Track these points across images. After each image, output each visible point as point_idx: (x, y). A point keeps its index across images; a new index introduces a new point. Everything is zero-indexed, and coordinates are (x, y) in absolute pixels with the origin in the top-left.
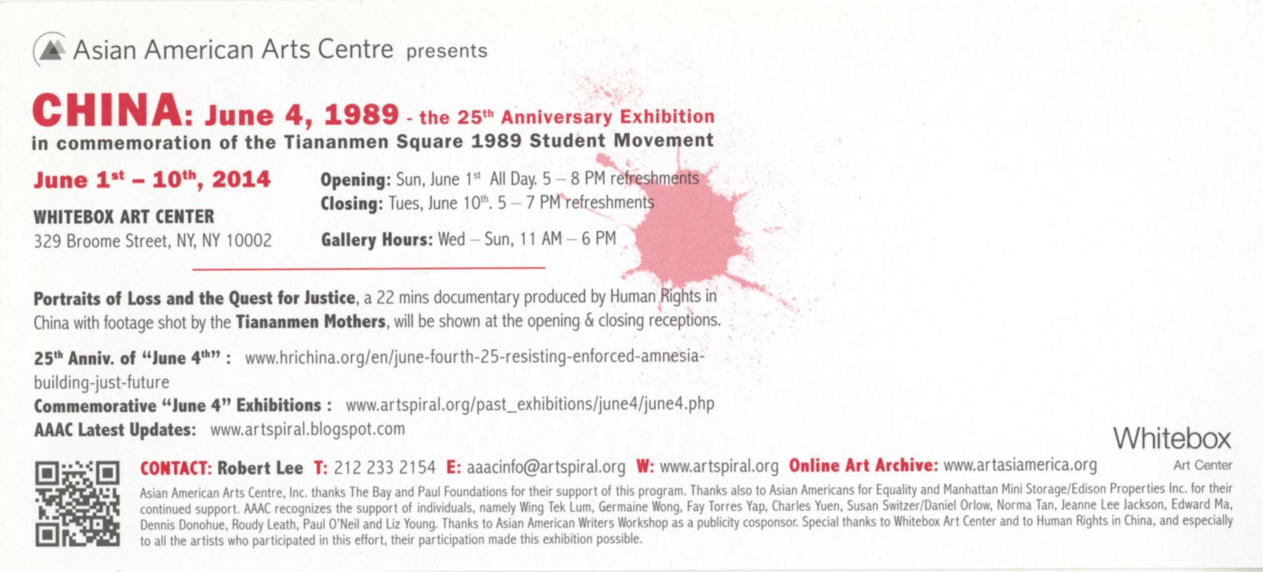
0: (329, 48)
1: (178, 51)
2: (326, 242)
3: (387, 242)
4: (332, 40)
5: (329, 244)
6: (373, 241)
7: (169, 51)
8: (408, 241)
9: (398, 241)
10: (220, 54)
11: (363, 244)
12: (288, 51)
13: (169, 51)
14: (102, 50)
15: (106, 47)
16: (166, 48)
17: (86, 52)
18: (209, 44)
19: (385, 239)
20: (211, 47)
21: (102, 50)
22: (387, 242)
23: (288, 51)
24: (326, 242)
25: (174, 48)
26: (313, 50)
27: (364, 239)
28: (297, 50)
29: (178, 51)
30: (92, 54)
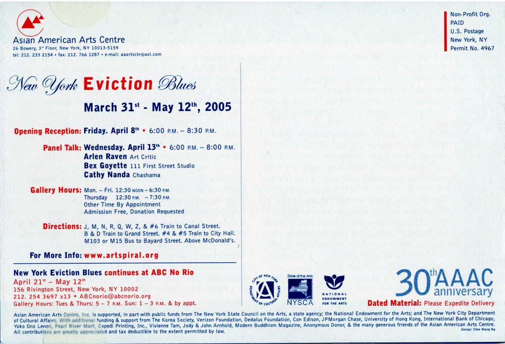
2: (33, 191)
3: (61, 191)
5: (34, 192)
6: (54, 190)
8: (70, 191)
9: (66, 191)
11: (49, 192)
14: (23, 40)
17: (17, 41)
19: (60, 190)
21: (23, 40)
22: (61, 191)
24: (33, 191)
27: (50, 189)
30: (19, 41)
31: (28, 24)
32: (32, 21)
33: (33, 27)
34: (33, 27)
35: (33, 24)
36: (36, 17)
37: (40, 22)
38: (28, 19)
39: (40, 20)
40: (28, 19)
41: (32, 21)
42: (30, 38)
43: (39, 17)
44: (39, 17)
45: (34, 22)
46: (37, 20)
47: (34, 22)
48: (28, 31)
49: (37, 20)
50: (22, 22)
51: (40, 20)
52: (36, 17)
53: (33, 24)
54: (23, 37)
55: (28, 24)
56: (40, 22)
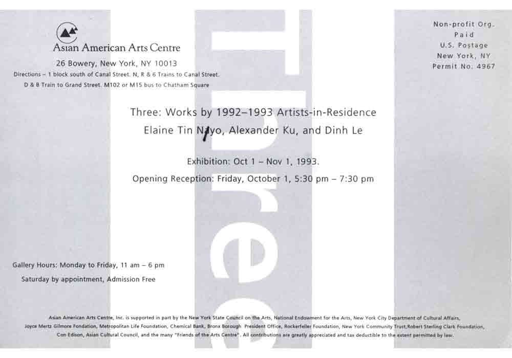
0: (154, 47)
1: (96, 48)
4: (157, 45)
7: (93, 48)
10: (112, 49)
12: (140, 49)
13: (93, 48)
15: (66, 47)
16: (91, 47)
18: (108, 46)
20: (108, 47)
23: (140, 49)
25: (94, 47)
26: (149, 48)
28: (143, 48)
29: (96, 48)
30: (61, 49)
31: (65, 34)
32: (69, 31)
33: (69, 36)
34: (69, 36)
35: (70, 35)
36: (72, 29)
37: (75, 33)
38: (65, 31)
39: (75, 31)
40: (65, 31)
41: (69, 31)
42: (72, 45)
43: (74, 28)
44: (74, 28)
45: (70, 33)
46: (73, 31)
47: (70, 33)
48: (64, 39)
49: (73, 31)
50: (61, 31)
51: (75, 31)
52: (72, 29)
53: (70, 35)
54: (65, 45)
55: (65, 34)
56: (75, 33)
